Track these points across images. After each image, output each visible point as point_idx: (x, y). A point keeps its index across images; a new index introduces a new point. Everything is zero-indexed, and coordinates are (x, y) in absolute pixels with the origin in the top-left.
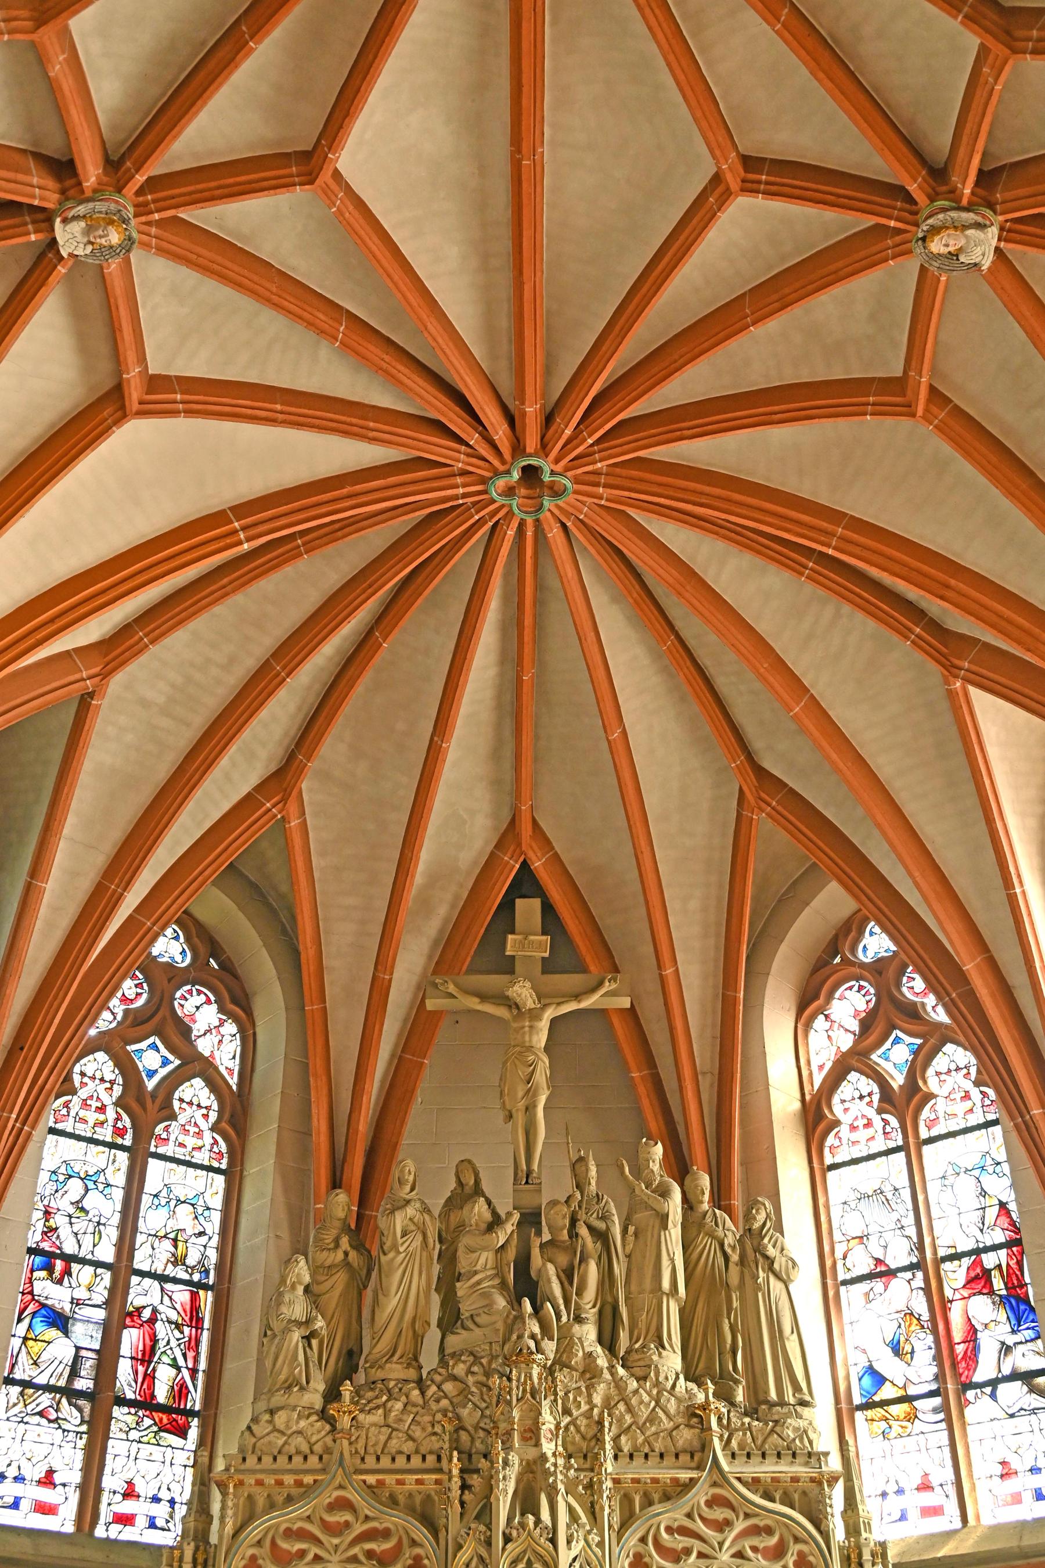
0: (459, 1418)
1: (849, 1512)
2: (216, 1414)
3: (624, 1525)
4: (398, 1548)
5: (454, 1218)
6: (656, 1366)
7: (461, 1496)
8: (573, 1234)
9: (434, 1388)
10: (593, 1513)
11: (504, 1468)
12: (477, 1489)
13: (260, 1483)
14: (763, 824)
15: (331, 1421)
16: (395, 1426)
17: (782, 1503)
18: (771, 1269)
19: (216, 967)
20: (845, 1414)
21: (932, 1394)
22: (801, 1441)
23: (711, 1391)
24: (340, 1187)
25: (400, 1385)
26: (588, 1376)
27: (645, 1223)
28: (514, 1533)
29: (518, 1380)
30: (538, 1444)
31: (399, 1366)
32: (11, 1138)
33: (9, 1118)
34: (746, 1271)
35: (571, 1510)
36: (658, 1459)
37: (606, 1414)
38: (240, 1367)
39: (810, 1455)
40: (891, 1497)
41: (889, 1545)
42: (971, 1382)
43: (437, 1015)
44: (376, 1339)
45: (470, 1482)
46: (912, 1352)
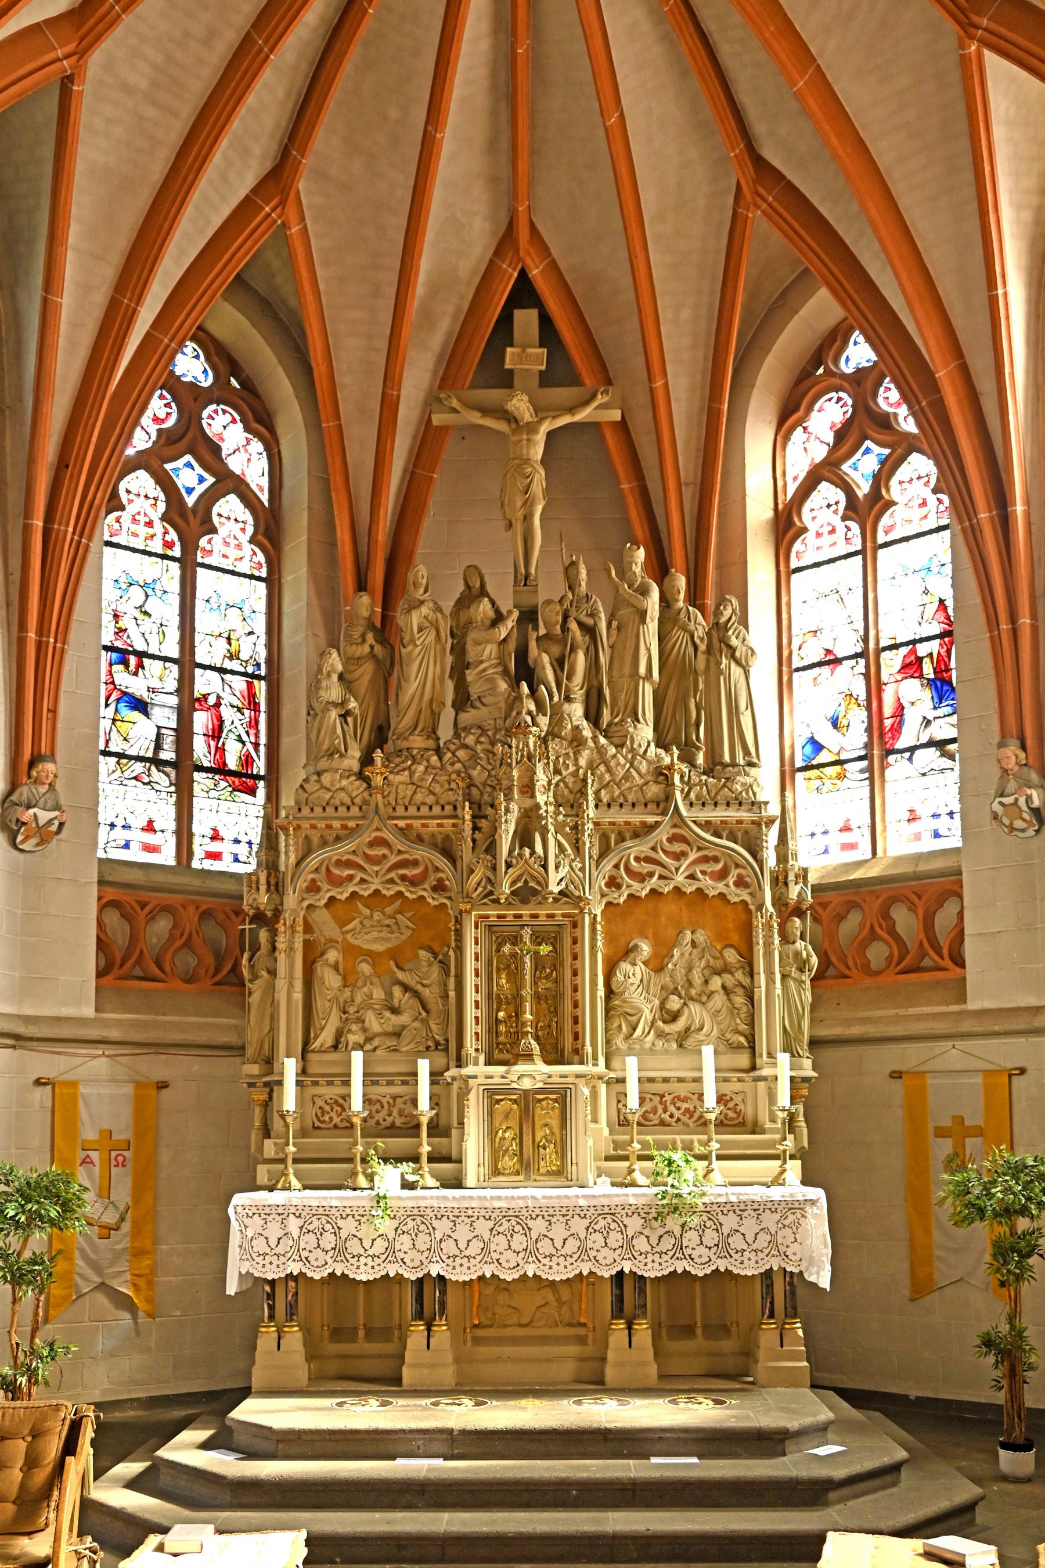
0: (470, 777)
1: (781, 846)
3: (602, 856)
4: (425, 873)
5: (463, 618)
8: (565, 629)
9: (449, 755)
10: (578, 849)
11: (505, 814)
12: (485, 830)
13: (313, 827)
14: (758, 223)
15: (367, 780)
16: (419, 784)
17: (727, 839)
18: (733, 656)
19: (238, 386)
22: (747, 794)
24: (365, 590)
26: (575, 744)
32: (72, 550)
33: (66, 532)
34: (711, 659)
35: (560, 846)
39: (753, 804)
43: (443, 430)
45: (480, 825)
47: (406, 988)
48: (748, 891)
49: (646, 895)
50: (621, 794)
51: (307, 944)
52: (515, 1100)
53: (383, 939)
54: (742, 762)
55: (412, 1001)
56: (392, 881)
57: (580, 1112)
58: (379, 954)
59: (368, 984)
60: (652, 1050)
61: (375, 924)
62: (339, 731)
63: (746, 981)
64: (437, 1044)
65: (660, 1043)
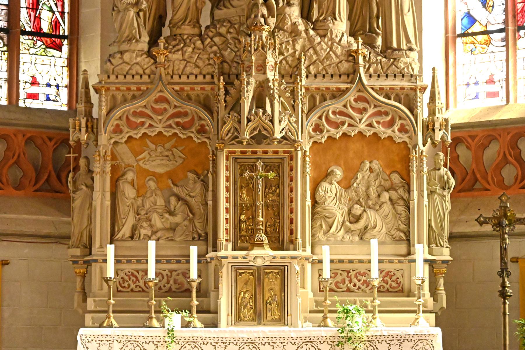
0: (222, 56)
1: (431, 104)
2: (78, 38)
3: (311, 110)
4: (192, 122)
6: (331, 30)
7: (225, 98)
13: (118, 89)
15: (154, 58)
16: (188, 60)
17: (395, 100)
20: (450, 39)
21: (501, 31)
23: (360, 43)
25: (190, 38)
26: (293, 35)
28: (252, 118)
29: (255, 40)
30: (265, 73)
31: (188, 27)
36: (330, 78)
37: (302, 55)
39: (412, 76)
40: (472, 86)
41: (449, 120)
42: (523, 26)
44: (175, 11)
46: (493, 6)
47: (179, 198)
48: (407, 135)
49: (340, 137)
50: (324, 68)
51: (113, 166)
52: (252, 273)
53: (164, 165)
54: (405, 48)
55: (183, 207)
56: (170, 126)
57: (293, 281)
58: (161, 175)
59: (154, 195)
60: (342, 241)
61: (158, 154)
62: (136, 25)
63: (406, 196)
64: (200, 236)
65: (347, 237)
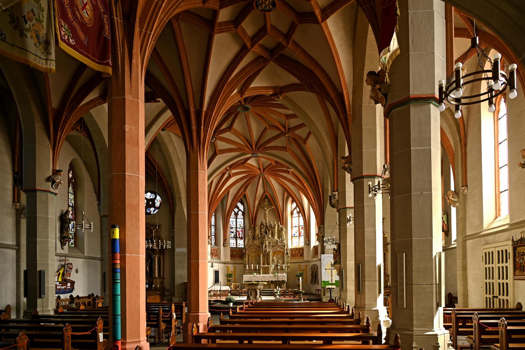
20: (292, 237)
27: (274, 227)
38: (246, 235)
